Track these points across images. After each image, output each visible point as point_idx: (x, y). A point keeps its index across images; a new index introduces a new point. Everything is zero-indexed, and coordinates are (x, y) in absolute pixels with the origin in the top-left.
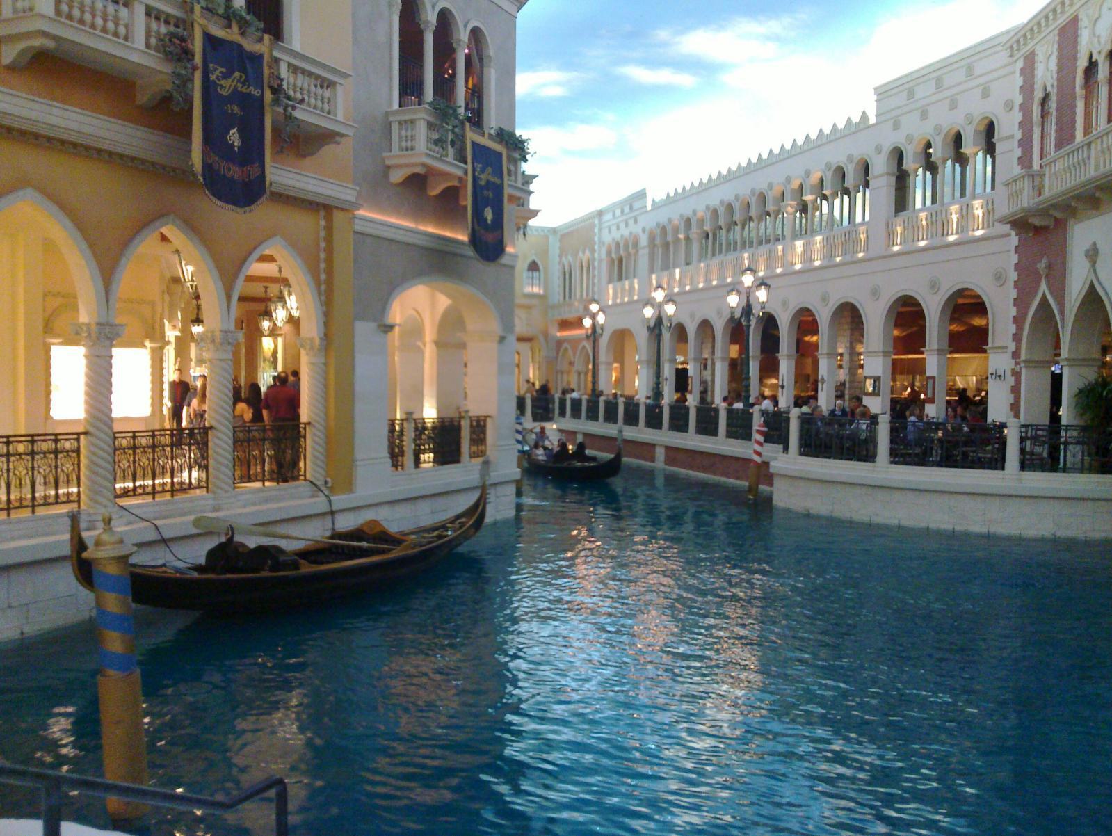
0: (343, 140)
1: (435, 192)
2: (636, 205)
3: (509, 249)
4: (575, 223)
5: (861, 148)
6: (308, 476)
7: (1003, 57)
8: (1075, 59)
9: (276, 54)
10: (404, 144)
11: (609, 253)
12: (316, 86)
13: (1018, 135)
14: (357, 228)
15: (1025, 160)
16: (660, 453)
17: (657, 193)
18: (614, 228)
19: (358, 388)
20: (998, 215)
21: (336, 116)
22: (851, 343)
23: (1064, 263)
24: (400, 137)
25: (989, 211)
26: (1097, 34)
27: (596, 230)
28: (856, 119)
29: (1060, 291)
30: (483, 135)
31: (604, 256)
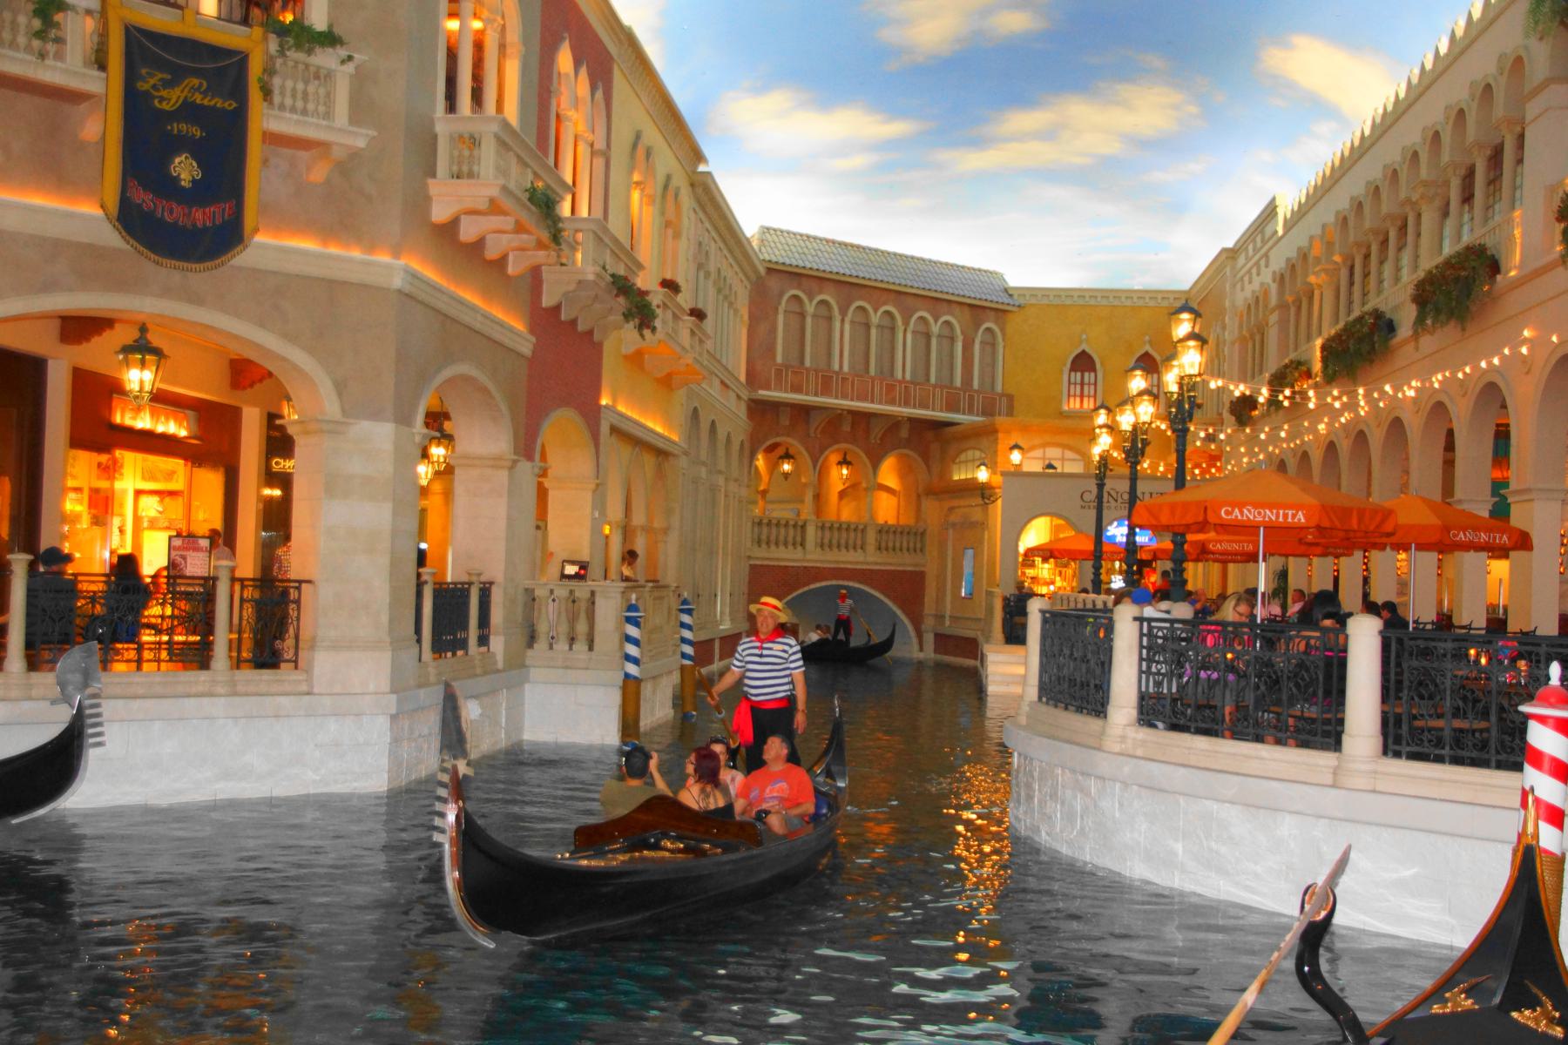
17: (1286, 206)
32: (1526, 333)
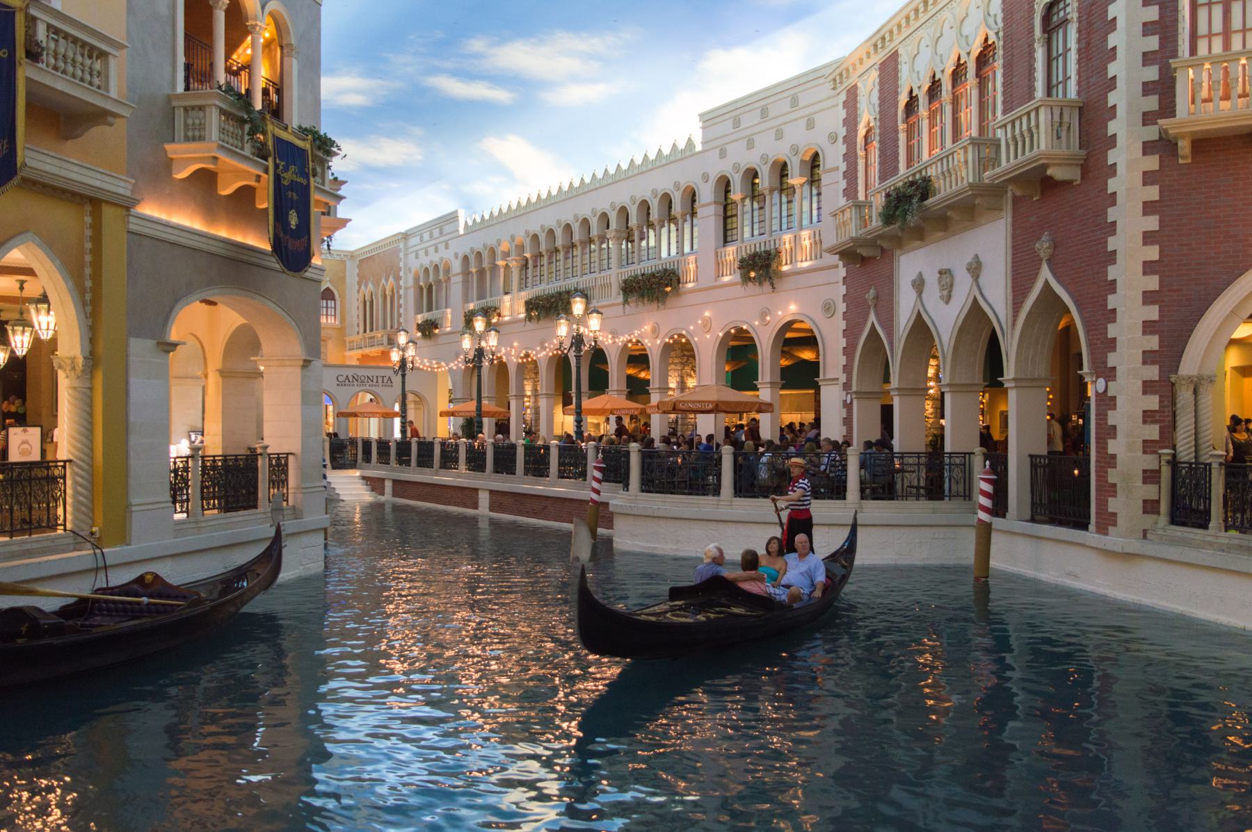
0: (117, 120)
1: (226, 191)
2: (447, 229)
3: (316, 261)
4: (377, 245)
5: (689, 175)
6: (69, 526)
7: (825, 90)
8: (897, 93)
9: (33, 12)
10: (190, 134)
11: (417, 279)
12: (83, 55)
13: (843, 167)
14: (132, 227)
15: (850, 192)
16: (484, 499)
18: (422, 253)
19: (132, 419)
20: (825, 246)
21: (108, 91)
22: (682, 377)
23: (891, 294)
24: (186, 125)
25: (817, 242)
26: (965, 33)
27: (402, 255)
28: (682, 145)
29: (888, 320)
30: (286, 128)
31: (411, 282)
32: (707, 314)
